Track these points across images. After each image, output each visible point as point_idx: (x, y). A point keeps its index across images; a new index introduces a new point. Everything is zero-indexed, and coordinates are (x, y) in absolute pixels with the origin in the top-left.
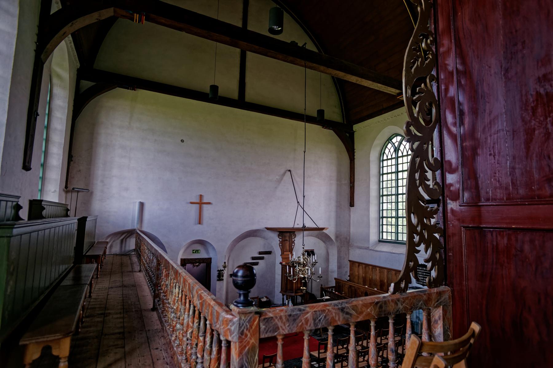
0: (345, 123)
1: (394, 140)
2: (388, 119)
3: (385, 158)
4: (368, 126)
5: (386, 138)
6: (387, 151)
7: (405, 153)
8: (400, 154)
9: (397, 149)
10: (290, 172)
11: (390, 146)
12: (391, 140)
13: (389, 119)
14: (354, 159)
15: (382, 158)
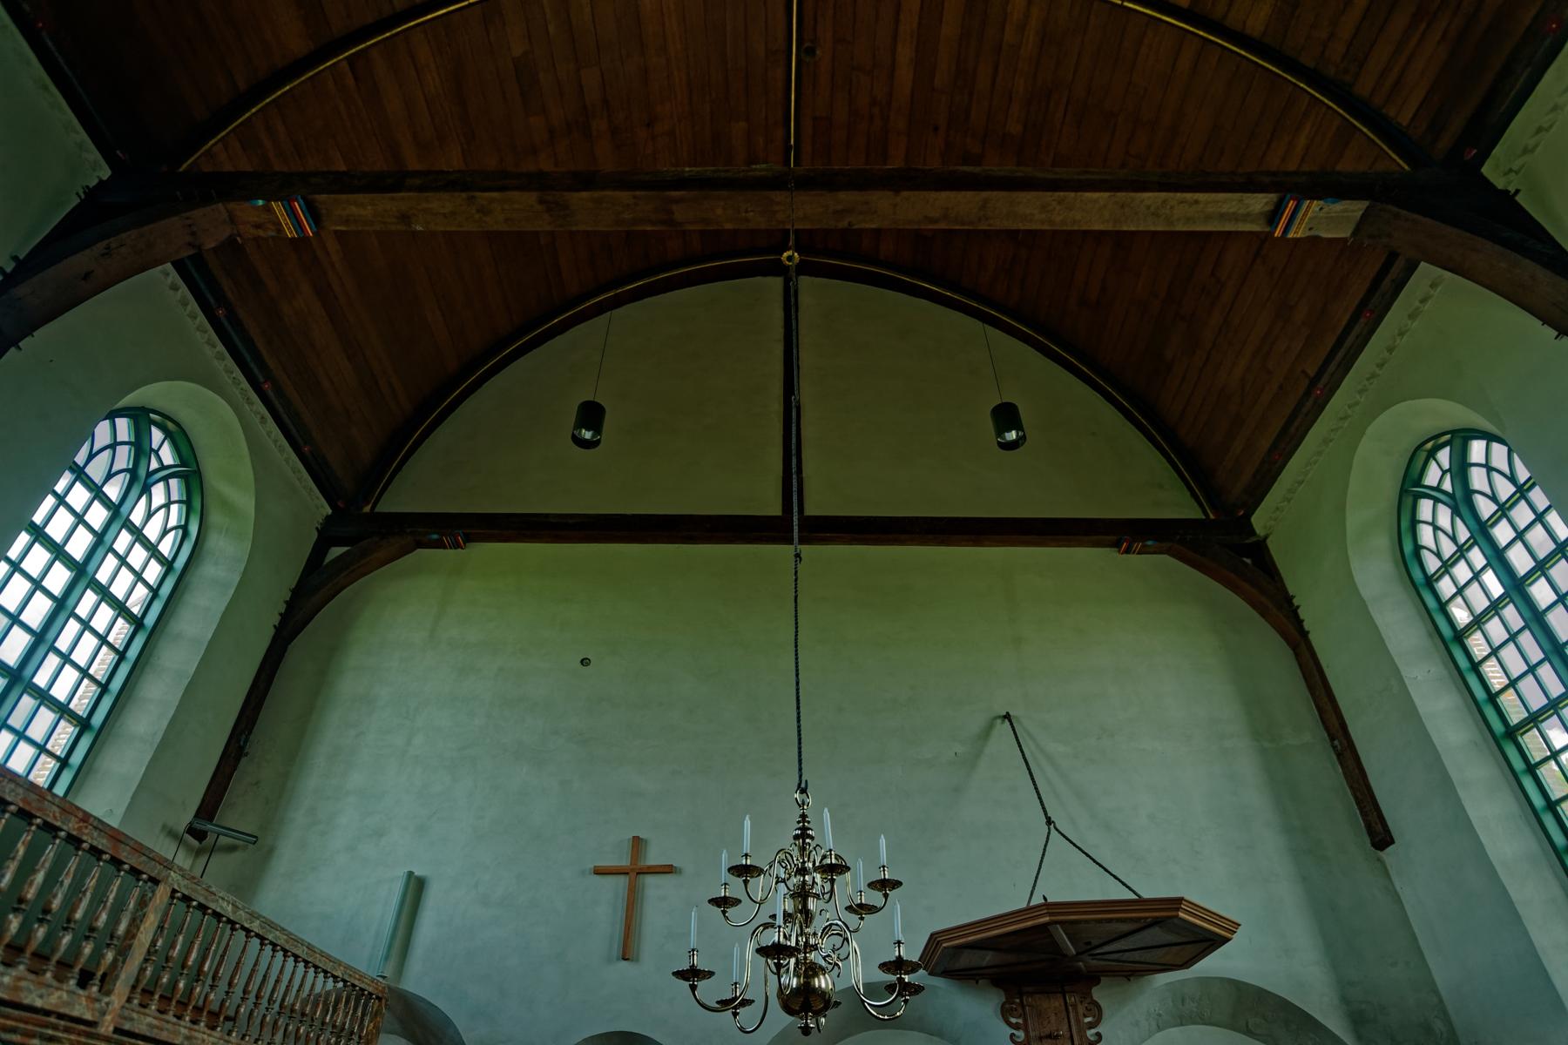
0: (1212, 516)
1: (1432, 476)
2: (1350, 407)
3: (1432, 564)
4: (1300, 483)
5: (1389, 486)
6: (1426, 535)
7: (1505, 490)
8: (1486, 508)
9: (1459, 495)
10: (1010, 721)
11: (1425, 508)
12: (1418, 483)
13: (1357, 403)
14: (1304, 634)
15: (1417, 575)
